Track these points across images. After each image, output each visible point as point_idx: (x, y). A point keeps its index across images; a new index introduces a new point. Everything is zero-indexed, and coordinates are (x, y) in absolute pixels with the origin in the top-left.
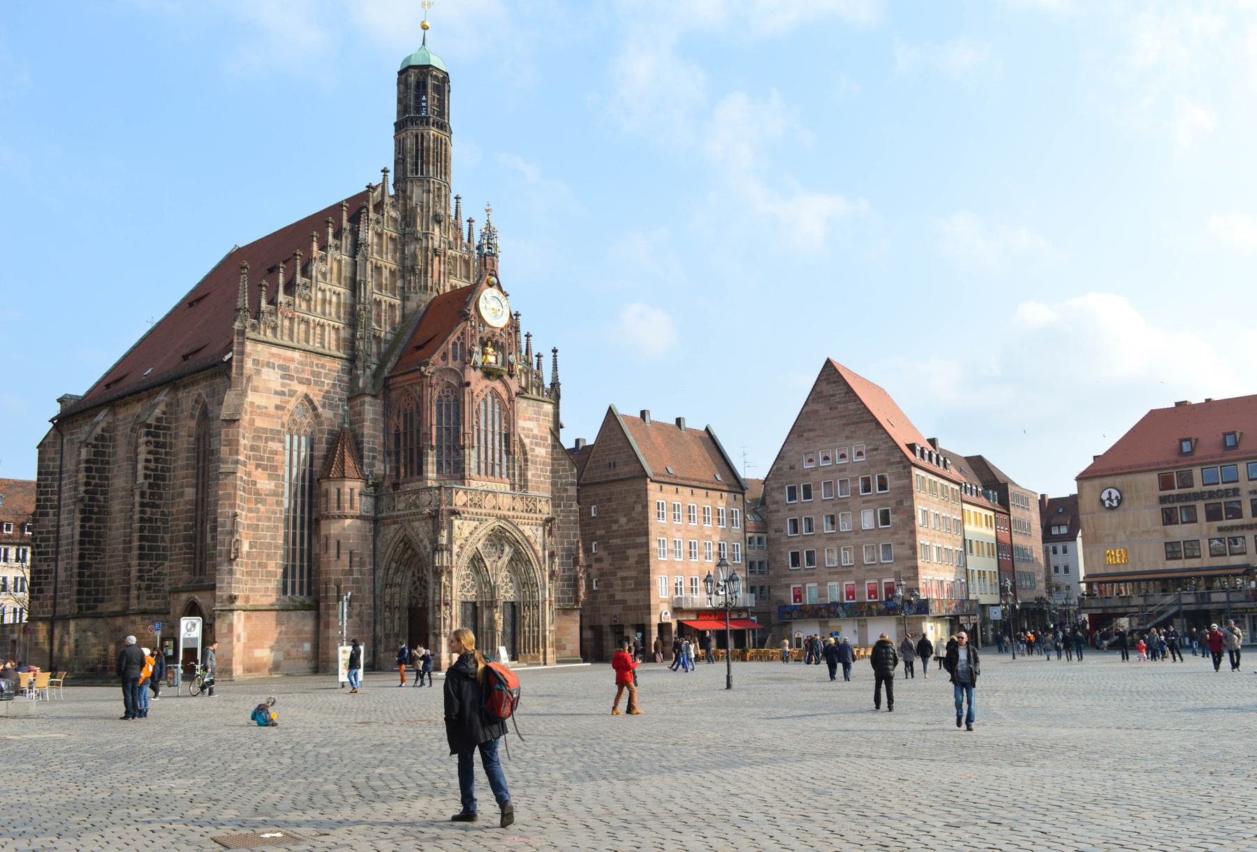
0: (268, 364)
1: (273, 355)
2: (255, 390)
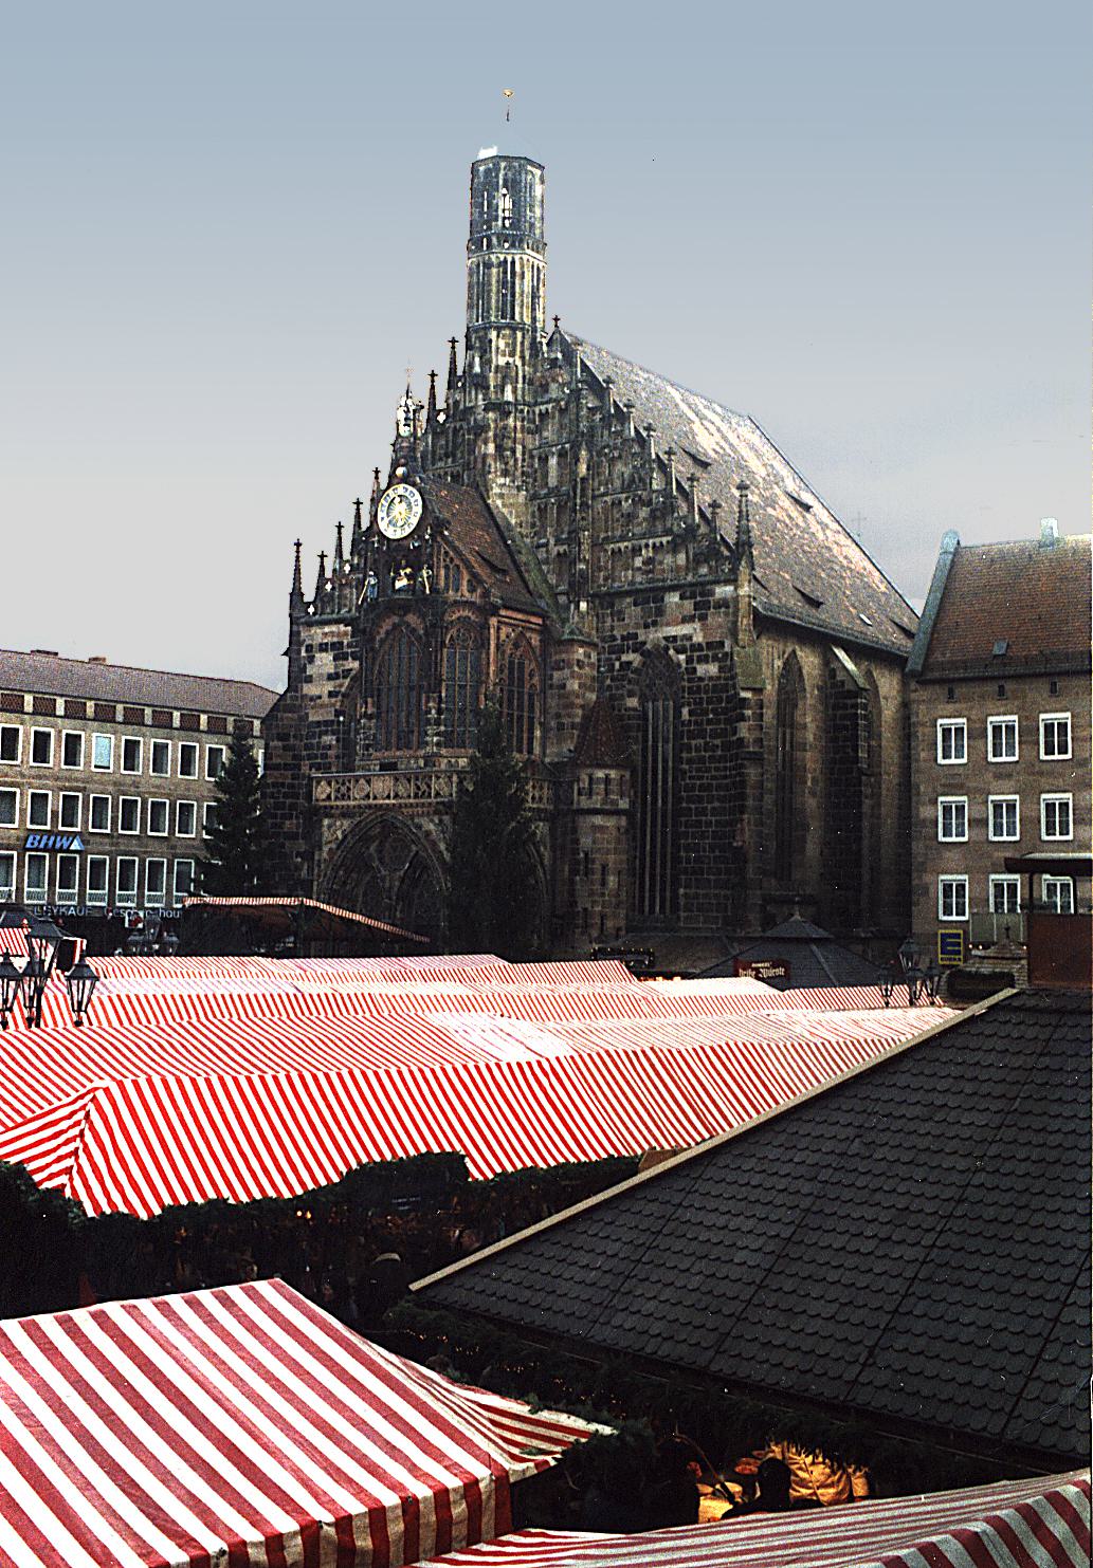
0: (323, 648)
1: (325, 634)
2: (309, 680)
